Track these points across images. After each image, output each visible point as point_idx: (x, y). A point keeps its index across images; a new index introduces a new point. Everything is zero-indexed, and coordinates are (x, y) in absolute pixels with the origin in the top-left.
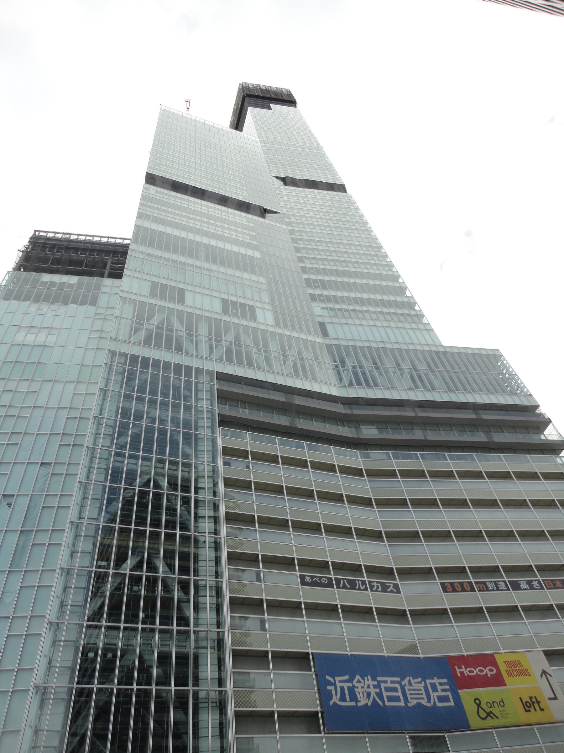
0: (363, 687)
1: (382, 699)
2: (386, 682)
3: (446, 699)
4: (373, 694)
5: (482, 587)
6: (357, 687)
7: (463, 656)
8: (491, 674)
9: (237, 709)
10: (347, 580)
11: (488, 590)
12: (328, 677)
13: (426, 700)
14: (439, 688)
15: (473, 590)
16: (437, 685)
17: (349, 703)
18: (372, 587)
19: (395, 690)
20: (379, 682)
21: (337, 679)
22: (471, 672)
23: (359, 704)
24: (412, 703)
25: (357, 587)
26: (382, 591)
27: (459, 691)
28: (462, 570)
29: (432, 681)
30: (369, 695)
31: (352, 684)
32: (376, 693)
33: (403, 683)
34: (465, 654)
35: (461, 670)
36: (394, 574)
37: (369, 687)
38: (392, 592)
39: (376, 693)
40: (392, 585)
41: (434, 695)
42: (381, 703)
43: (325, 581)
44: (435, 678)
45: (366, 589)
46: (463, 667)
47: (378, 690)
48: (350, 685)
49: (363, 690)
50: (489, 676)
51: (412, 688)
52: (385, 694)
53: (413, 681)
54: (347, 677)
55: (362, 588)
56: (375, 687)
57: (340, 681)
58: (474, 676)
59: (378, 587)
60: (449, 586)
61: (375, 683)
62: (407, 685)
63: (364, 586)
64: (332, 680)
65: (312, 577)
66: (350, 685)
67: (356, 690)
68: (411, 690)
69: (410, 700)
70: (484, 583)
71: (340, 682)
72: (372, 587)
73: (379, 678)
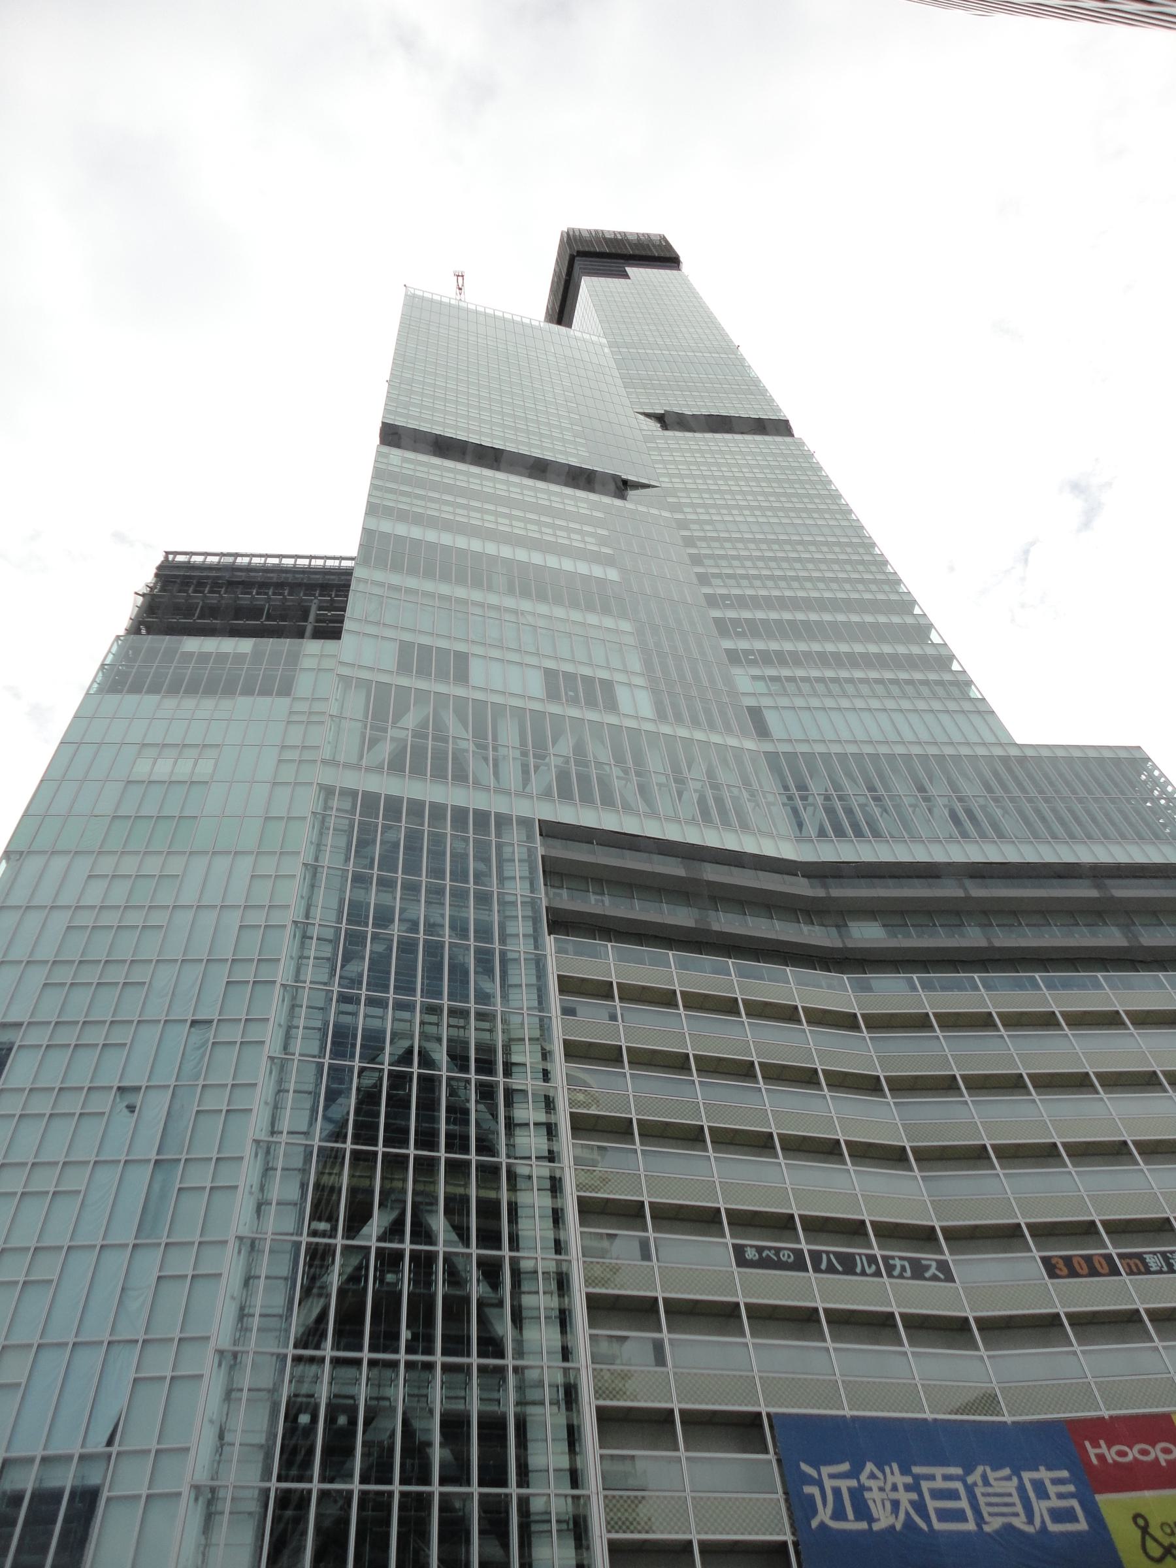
1: (926, 1517)
2: (932, 1478)
4: (905, 1505)
5: (1136, 1265)
6: (870, 1489)
7: (1101, 1419)
8: (1167, 1461)
9: (614, 1536)
10: (835, 1253)
11: (1148, 1271)
12: (804, 1467)
14: (1052, 1490)
15: (1115, 1272)
16: (1048, 1483)
17: (853, 1525)
18: (890, 1269)
19: (953, 1495)
20: (917, 1478)
21: (826, 1470)
22: (1122, 1454)
23: (876, 1527)
24: (993, 1525)
25: (858, 1270)
26: (913, 1277)
27: (1098, 1497)
28: (1087, 1230)
29: (1035, 1475)
30: (896, 1504)
31: (859, 1481)
32: (912, 1502)
33: (970, 1480)
34: (1106, 1414)
35: (1098, 1451)
36: (936, 1239)
37: (895, 1488)
38: (935, 1278)
39: (912, 1502)
40: (934, 1264)
41: (1041, 1507)
42: (923, 1525)
43: (789, 1256)
44: (1042, 1468)
45: (878, 1274)
46: (1102, 1442)
47: (914, 1496)
48: (853, 1483)
50: (1163, 1464)
51: (990, 1490)
52: (932, 1505)
53: (991, 1475)
54: (845, 1467)
55: (868, 1271)
56: (908, 1488)
57: (832, 1476)
58: (1130, 1463)
59: (903, 1268)
60: (1061, 1264)
61: (909, 1480)
62: (980, 1483)
63: (874, 1267)
64: (814, 1473)
65: (760, 1250)
66: (853, 1483)
67: (867, 1495)
68: (989, 1495)
70: (1140, 1256)
71: (831, 1478)
72: (890, 1269)
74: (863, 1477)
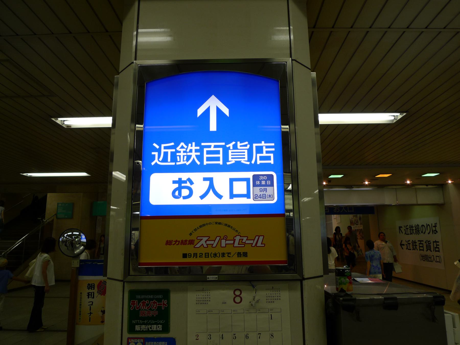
0: (184, 152)
2: (210, 147)
3: (269, 158)
6: (180, 152)
12: (155, 145)
13: (246, 159)
14: (265, 149)
19: (218, 152)
21: (163, 146)
30: (189, 157)
37: (191, 151)
39: (196, 156)
42: (198, 163)
48: (174, 150)
49: (185, 154)
52: (205, 156)
54: (173, 144)
56: (196, 151)
57: (165, 148)
61: (198, 148)
62: (231, 148)
64: (157, 147)
66: (174, 150)
69: (230, 159)
73: (203, 144)
74: (178, 149)
